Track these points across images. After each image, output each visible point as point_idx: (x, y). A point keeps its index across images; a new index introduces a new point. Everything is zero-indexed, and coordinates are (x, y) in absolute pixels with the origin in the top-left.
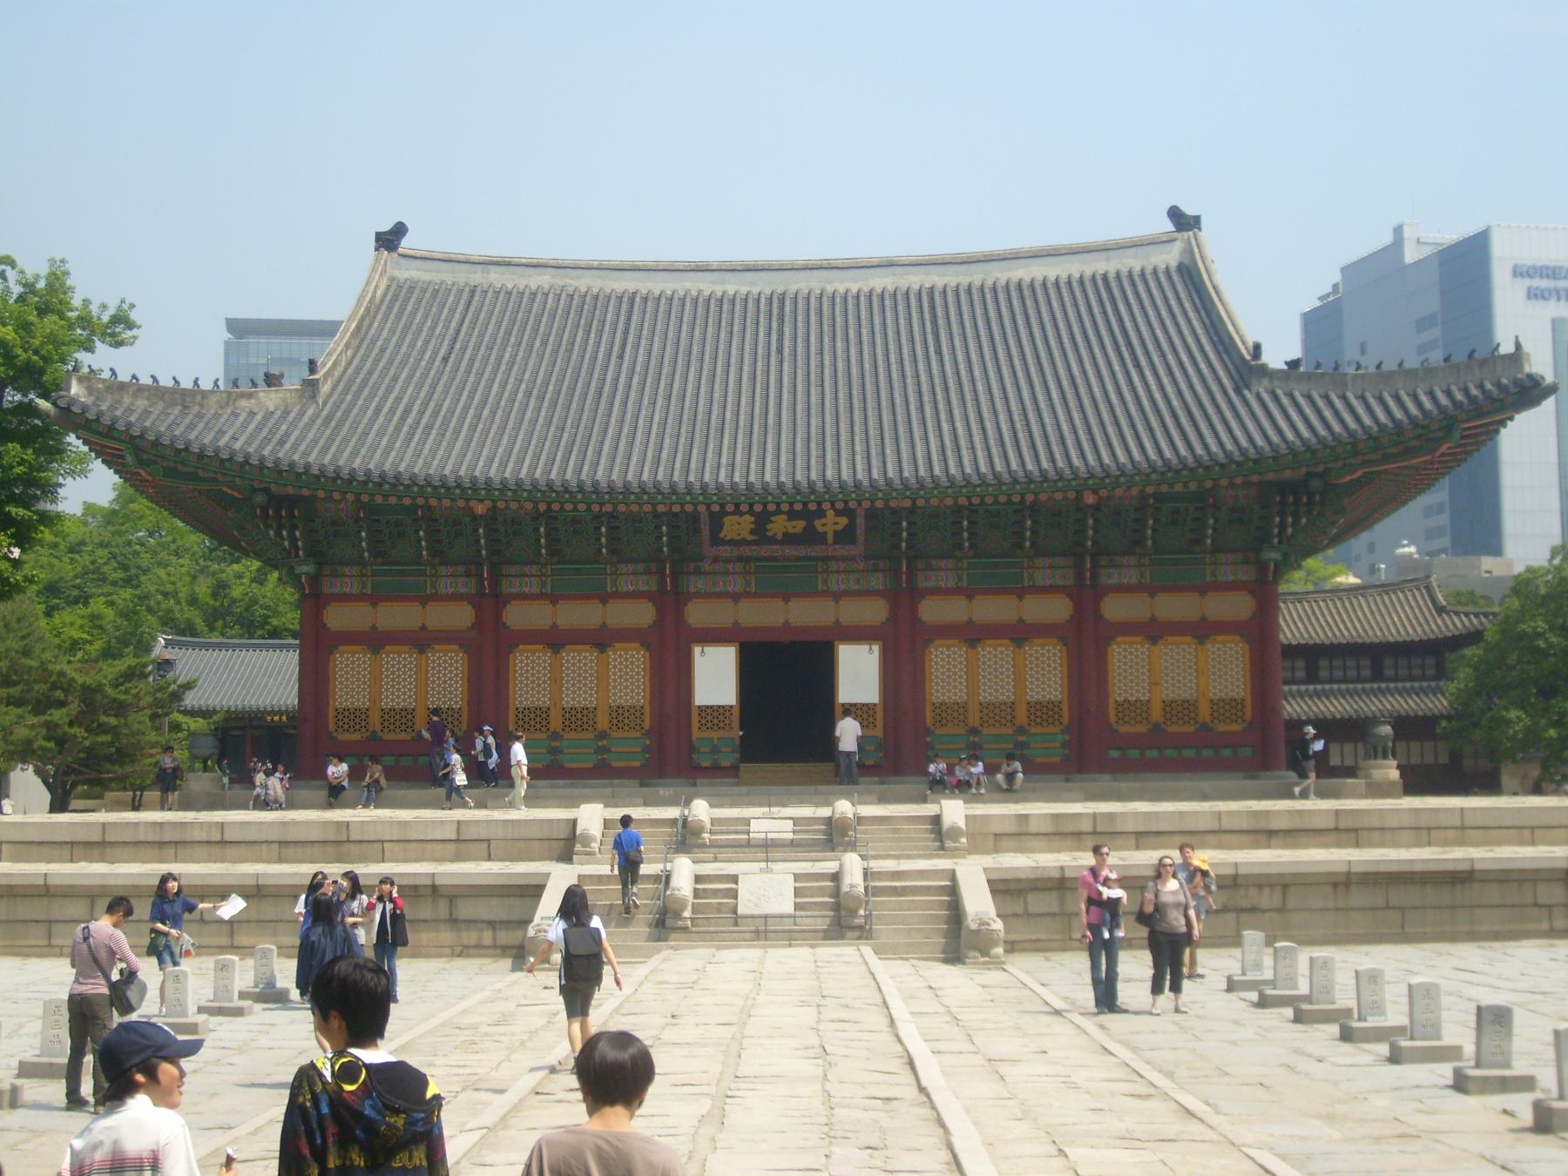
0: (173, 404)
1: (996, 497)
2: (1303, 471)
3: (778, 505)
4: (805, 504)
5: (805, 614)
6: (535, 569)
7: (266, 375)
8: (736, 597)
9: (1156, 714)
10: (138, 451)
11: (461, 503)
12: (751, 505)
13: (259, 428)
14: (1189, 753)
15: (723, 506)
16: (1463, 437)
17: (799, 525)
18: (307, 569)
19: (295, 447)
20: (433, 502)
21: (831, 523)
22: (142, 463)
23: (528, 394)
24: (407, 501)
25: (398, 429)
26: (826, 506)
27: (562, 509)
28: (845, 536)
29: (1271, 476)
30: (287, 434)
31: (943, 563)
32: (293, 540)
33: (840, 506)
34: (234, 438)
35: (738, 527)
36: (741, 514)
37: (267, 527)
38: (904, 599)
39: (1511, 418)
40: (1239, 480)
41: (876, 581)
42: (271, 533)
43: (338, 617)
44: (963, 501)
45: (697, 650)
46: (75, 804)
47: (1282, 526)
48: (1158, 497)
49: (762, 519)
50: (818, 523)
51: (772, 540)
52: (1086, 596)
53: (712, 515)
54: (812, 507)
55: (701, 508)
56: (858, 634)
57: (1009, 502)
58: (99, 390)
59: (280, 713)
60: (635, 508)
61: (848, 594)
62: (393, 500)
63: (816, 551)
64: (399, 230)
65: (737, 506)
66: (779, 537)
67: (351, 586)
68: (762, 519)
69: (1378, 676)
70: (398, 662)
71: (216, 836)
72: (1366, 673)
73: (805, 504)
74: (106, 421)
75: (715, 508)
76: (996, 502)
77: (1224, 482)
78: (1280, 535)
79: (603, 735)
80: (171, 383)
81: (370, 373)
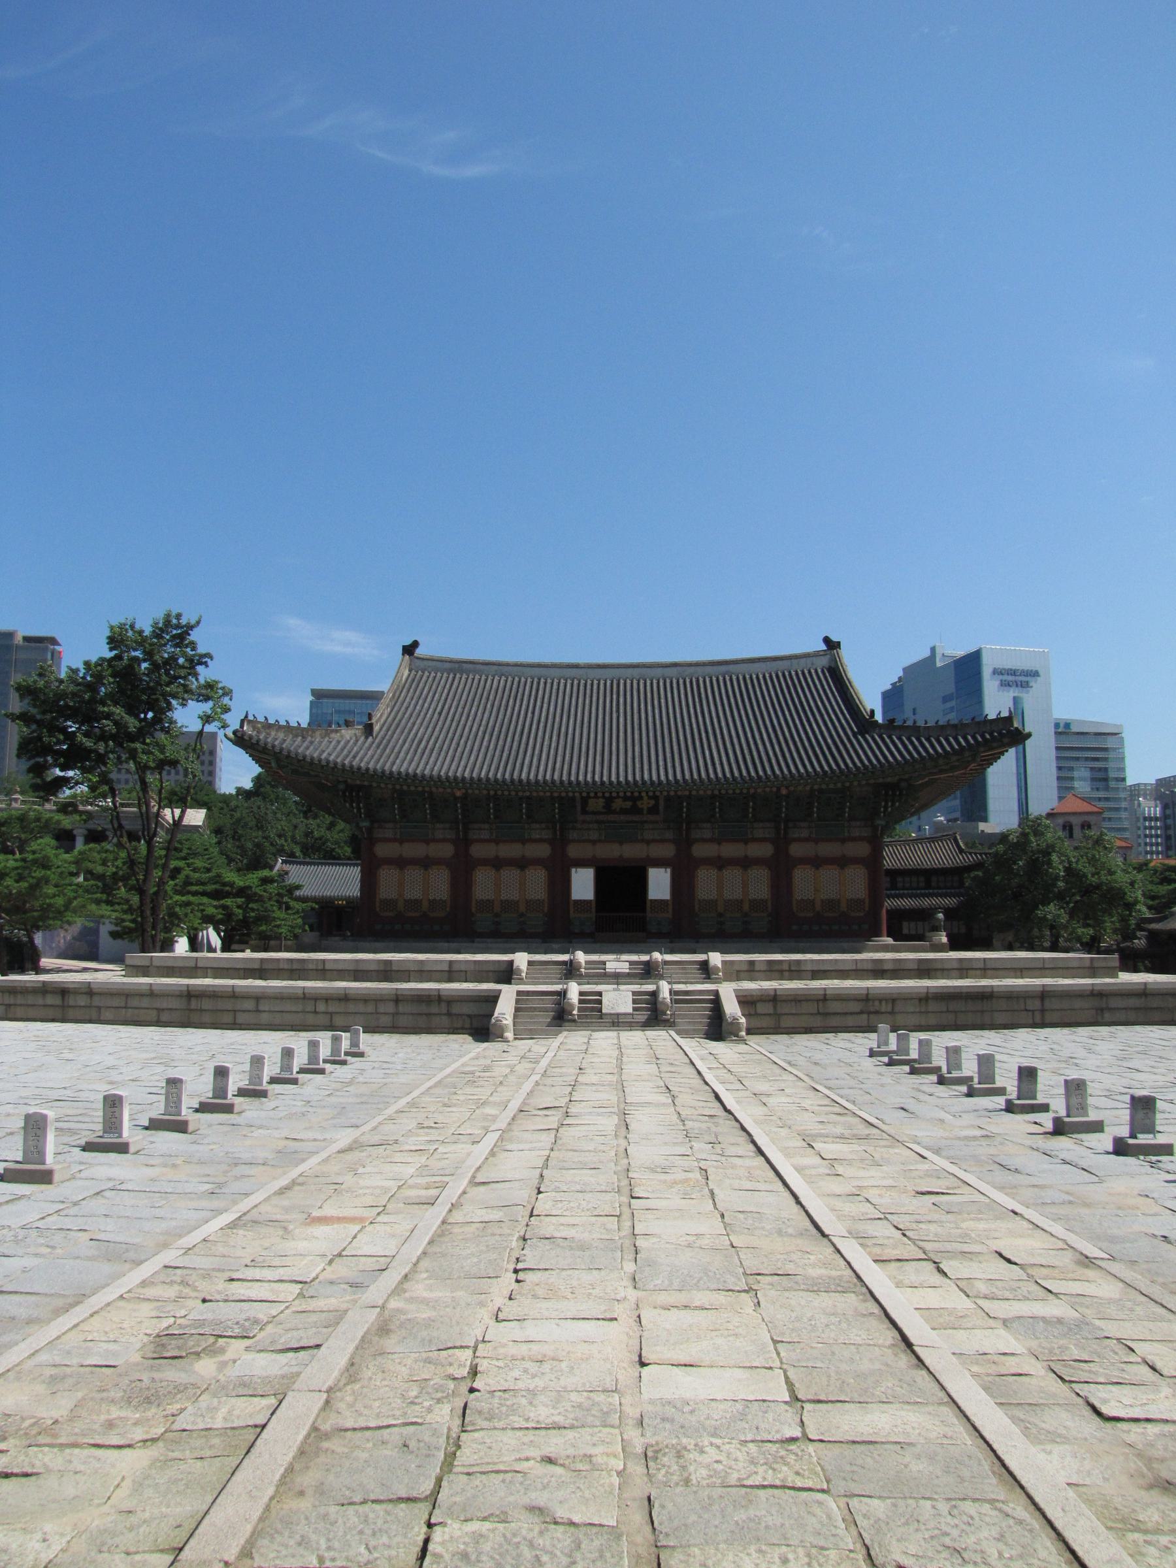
0: (297, 736)
1: (734, 790)
2: (897, 777)
3: (618, 793)
4: (632, 793)
5: (631, 851)
6: (486, 826)
7: (346, 721)
8: (594, 842)
9: (818, 907)
10: (278, 760)
11: (449, 790)
12: (603, 793)
13: (342, 750)
14: (835, 927)
15: (588, 793)
16: (982, 761)
17: (629, 804)
18: (365, 824)
19: (361, 760)
20: (434, 789)
21: (645, 804)
22: (280, 767)
23: (485, 733)
24: (420, 789)
25: (416, 751)
26: (644, 794)
27: (503, 794)
28: (653, 810)
29: (881, 780)
30: (357, 753)
31: (705, 825)
32: (359, 809)
33: (651, 794)
34: (330, 755)
35: (597, 804)
36: (598, 798)
37: (345, 801)
38: (684, 844)
39: (1007, 751)
40: (864, 782)
41: (669, 835)
42: (347, 805)
43: (382, 850)
44: (716, 792)
45: (573, 870)
46: (234, 947)
47: (886, 807)
48: (821, 791)
49: (609, 801)
50: (639, 803)
51: (614, 812)
52: (781, 843)
53: (582, 798)
54: (636, 794)
55: (577, 795)
56: (659, 863)
57: (741, 793)
58: (258, 729)
59: (342, 899)
60: (541, 794)
61: (654, 841)
62: (412, 788)
63: (636, 818)
64: (415, 644)
65: (596, 793)
66: (618, 810)
67: (389, 834)
68: (609, 801)
69: (928, 886)
70: (414, 875)
71: (320, 967)
72: (922, 884)
73: (632, 793)
74: (262, 743)
75: (584, 794)
76: (734, 793)
77: (856, 783)
78: (884, 812)
79: (522, 915)
80: (296, 725)
81: (400, 721)
